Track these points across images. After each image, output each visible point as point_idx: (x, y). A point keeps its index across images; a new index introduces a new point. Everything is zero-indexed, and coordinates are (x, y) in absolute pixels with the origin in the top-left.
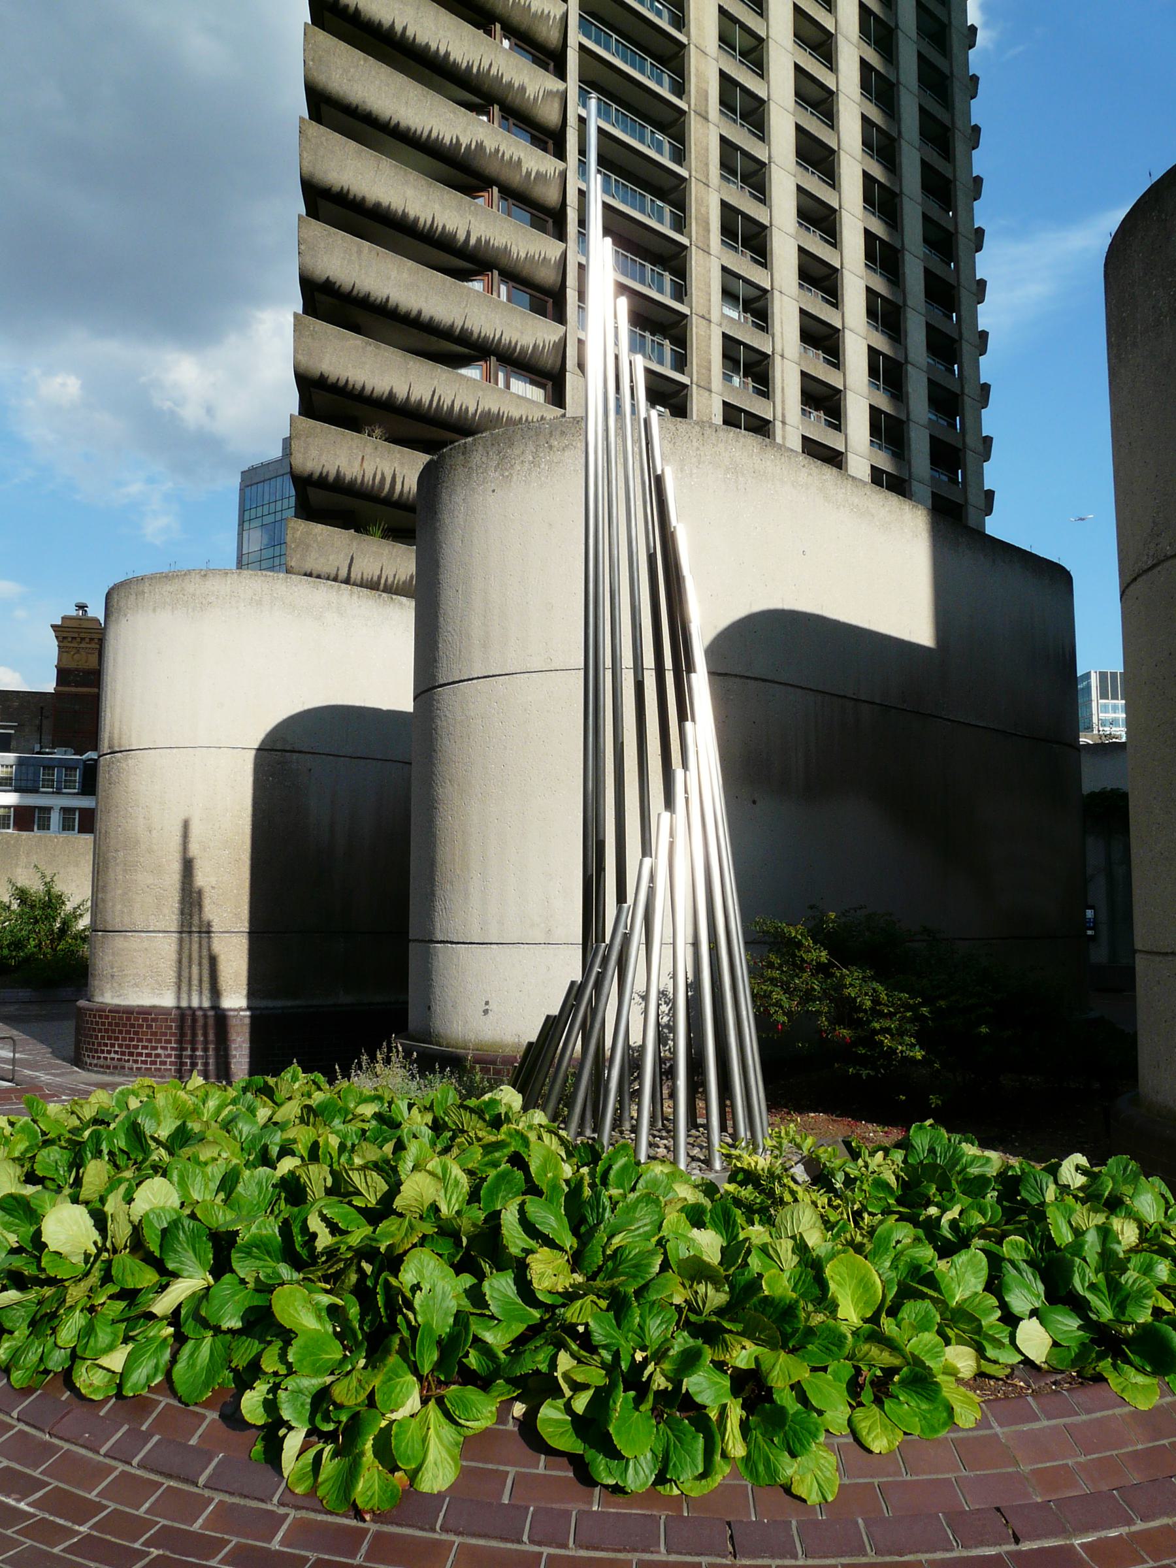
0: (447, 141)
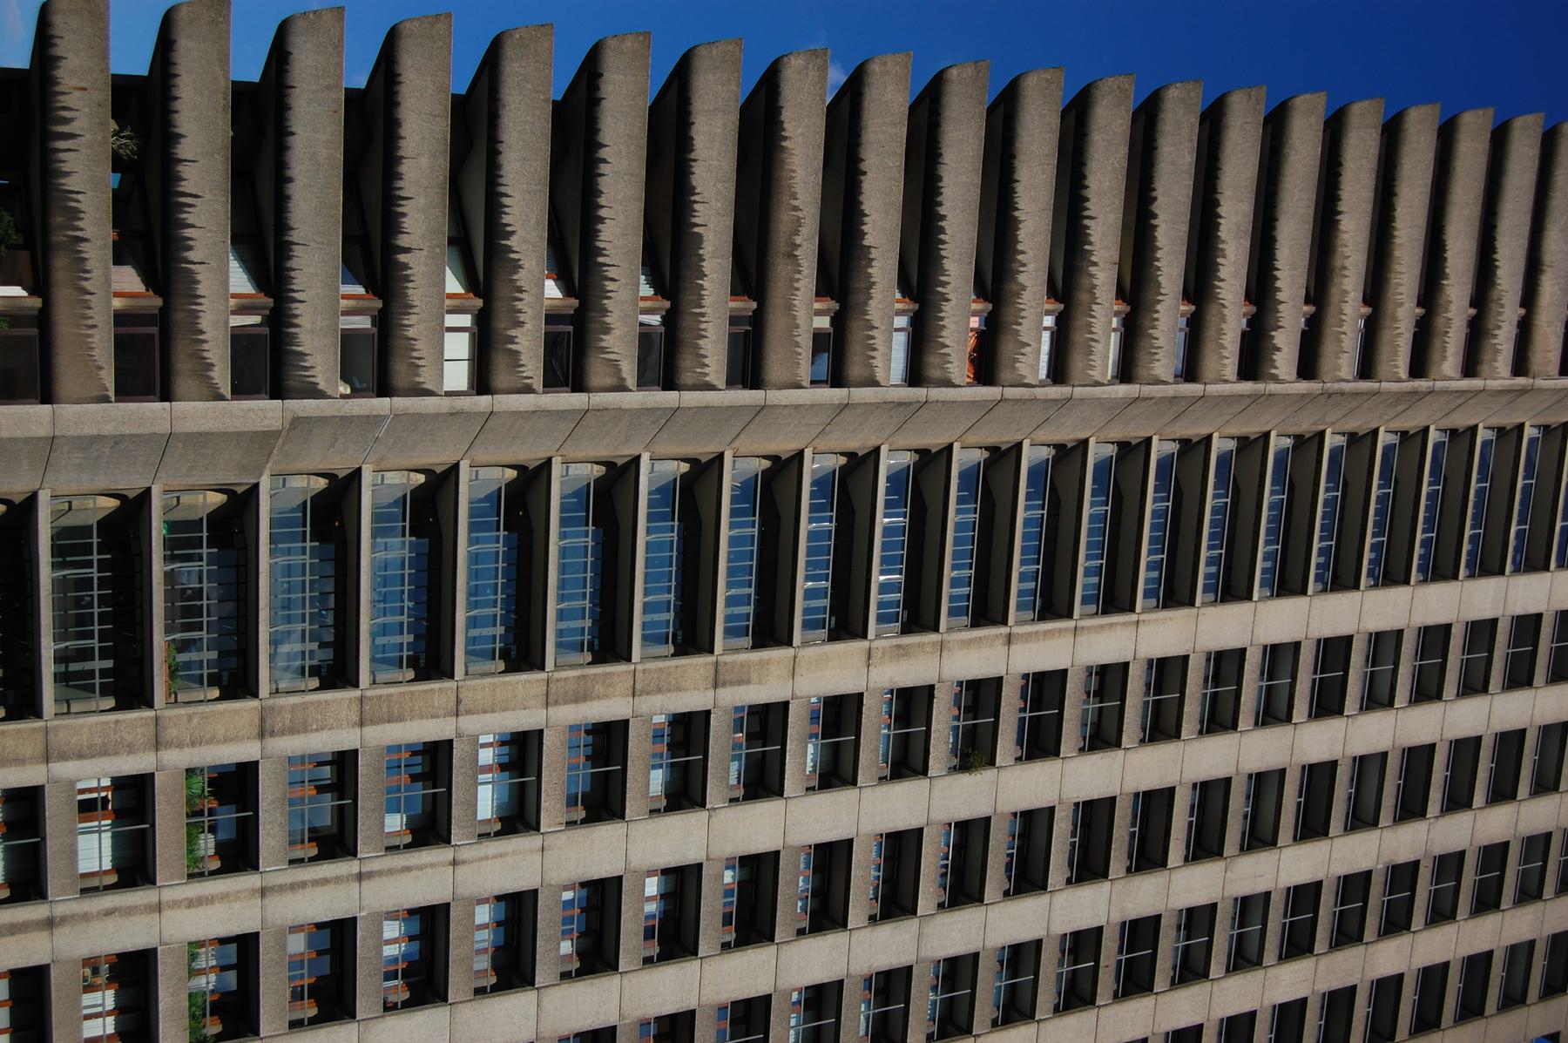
0: (506, 219)
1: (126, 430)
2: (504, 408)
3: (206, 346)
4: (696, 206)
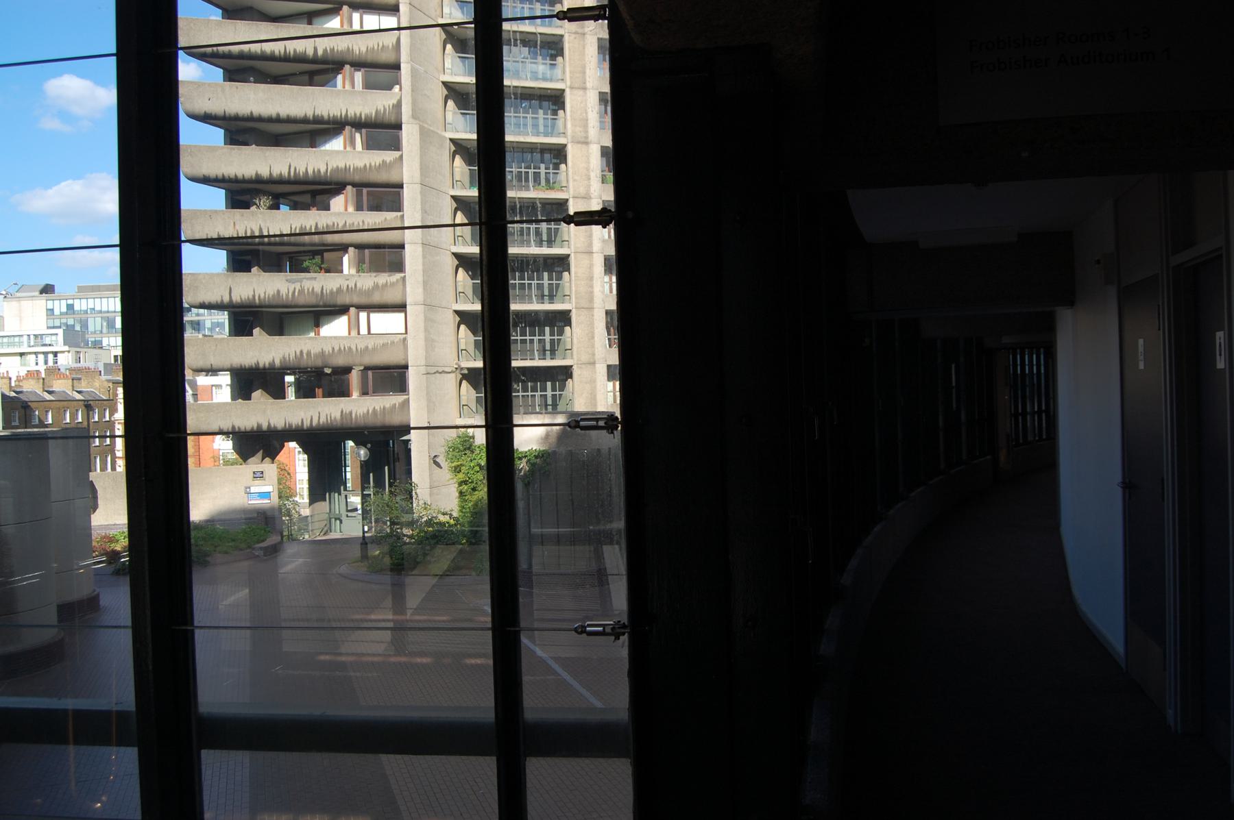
1: (419, 207)
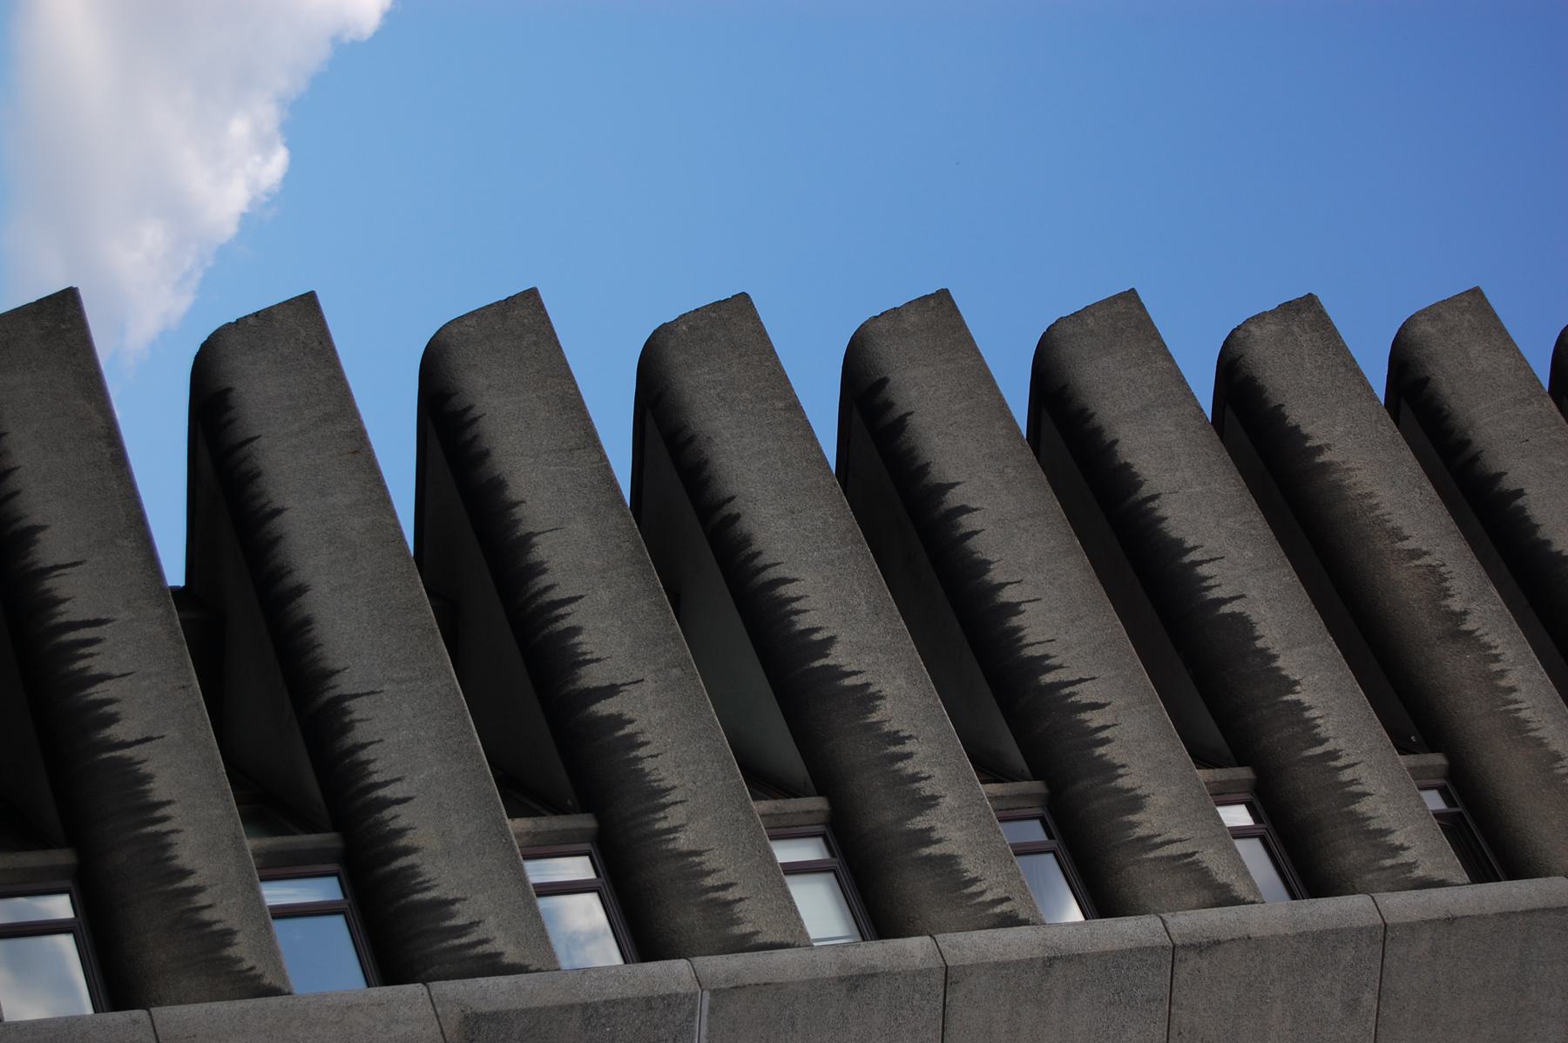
2: (970, 957)
3: (202, 899)
4: (1204, 570)
